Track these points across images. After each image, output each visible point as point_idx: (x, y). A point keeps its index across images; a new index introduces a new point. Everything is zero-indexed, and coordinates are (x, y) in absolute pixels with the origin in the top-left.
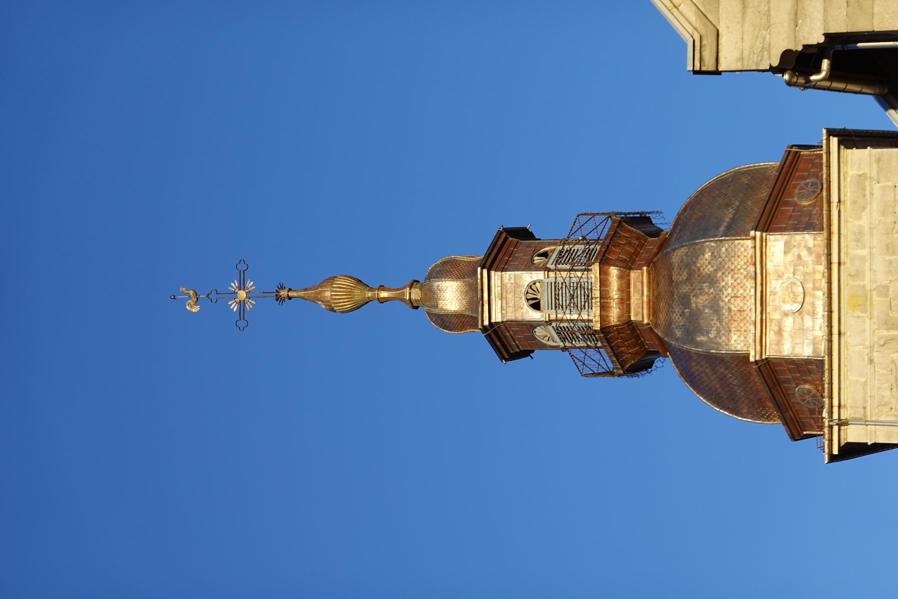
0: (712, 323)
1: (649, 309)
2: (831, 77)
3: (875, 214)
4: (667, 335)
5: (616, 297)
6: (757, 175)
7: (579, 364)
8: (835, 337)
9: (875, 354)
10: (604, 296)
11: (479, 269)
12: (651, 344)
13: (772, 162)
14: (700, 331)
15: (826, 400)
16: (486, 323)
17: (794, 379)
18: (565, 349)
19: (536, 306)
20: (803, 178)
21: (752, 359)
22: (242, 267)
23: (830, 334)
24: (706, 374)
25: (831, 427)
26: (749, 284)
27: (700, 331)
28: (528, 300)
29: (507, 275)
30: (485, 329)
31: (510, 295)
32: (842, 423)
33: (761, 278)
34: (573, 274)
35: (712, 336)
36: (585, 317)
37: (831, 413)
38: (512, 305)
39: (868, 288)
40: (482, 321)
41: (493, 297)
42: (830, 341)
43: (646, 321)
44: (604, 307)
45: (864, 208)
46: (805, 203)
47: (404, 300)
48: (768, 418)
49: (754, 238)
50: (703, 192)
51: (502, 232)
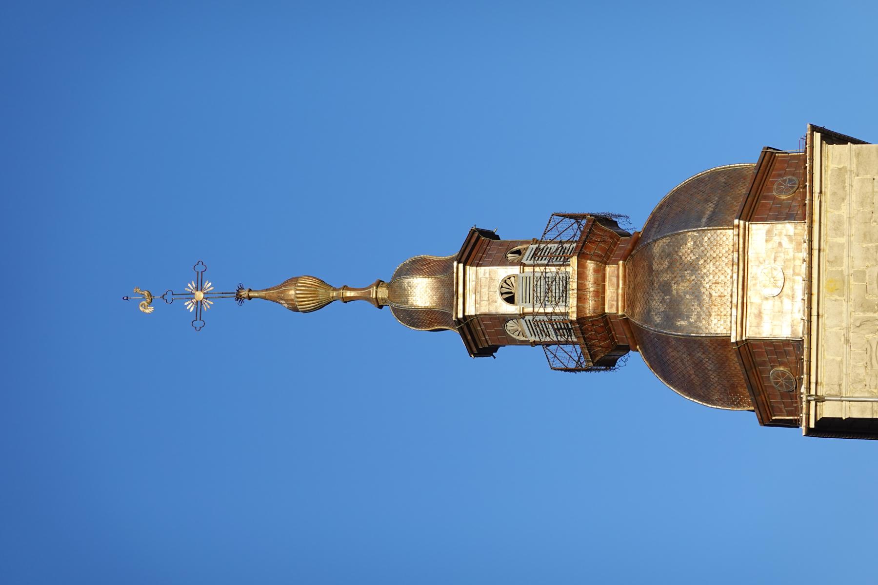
0: (693, 308)
1: (624, 301)
3: (854, 205)
4: (646, 322)
5: (592, 289)
6: (733, 176)
7: (551, 356)
8: (814, 318)
9: (851, 334)
11: (455, 263)
12: (622, 336)
13: (750, 160)
14: (680, 315)
15: (805, 377)
16: (460, 315)
17: (771, 361)
18: (534, 344)
19: (510, 300)
20: (780, 176)
21: (733, 340)
23: (810, 315)
24: (682, 361)
25: (809, 402)
28: (502, 294)
29: (481, 270)
30: (459, 321)
31: (483, 290)
32: (819, 400)
34: (548, 269)
35: (692, 320)
37: (809, 389)
38: (486, 298)
39: (846, 273)
40: (457, 313)
41: (467, 291)
42: (810, 321)
43: (620, 313)
44: (581, 299)
45: (843, 199)
46: (783, 197)
47: (369, 299)
48: (738, 405)
49: (738, 226)
50: (679, 191)
51: (474, 231)
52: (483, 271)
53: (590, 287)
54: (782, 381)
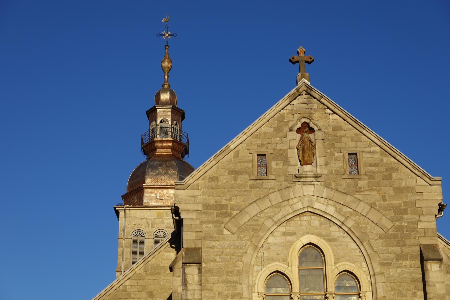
2: (176, 220)
8: (149, 208)
10: (164, 142)
14: (152, 169)
15: (131, 206)
19: (161, 122)
22: (175, 35)
23: (150, 207)
25: (123, 207)
26: (165, 184)
27: (152, 169)
29: (170, 113)
30: (155, 107)
31: (165, 114)
33: (166, 187)
36: (158, 136)
37: (128, 207)
42: (148, 207)
44: (160, 142)
48: (128, 189)
52: (170, 114)
53: (164, 145)
54: (133, 200)
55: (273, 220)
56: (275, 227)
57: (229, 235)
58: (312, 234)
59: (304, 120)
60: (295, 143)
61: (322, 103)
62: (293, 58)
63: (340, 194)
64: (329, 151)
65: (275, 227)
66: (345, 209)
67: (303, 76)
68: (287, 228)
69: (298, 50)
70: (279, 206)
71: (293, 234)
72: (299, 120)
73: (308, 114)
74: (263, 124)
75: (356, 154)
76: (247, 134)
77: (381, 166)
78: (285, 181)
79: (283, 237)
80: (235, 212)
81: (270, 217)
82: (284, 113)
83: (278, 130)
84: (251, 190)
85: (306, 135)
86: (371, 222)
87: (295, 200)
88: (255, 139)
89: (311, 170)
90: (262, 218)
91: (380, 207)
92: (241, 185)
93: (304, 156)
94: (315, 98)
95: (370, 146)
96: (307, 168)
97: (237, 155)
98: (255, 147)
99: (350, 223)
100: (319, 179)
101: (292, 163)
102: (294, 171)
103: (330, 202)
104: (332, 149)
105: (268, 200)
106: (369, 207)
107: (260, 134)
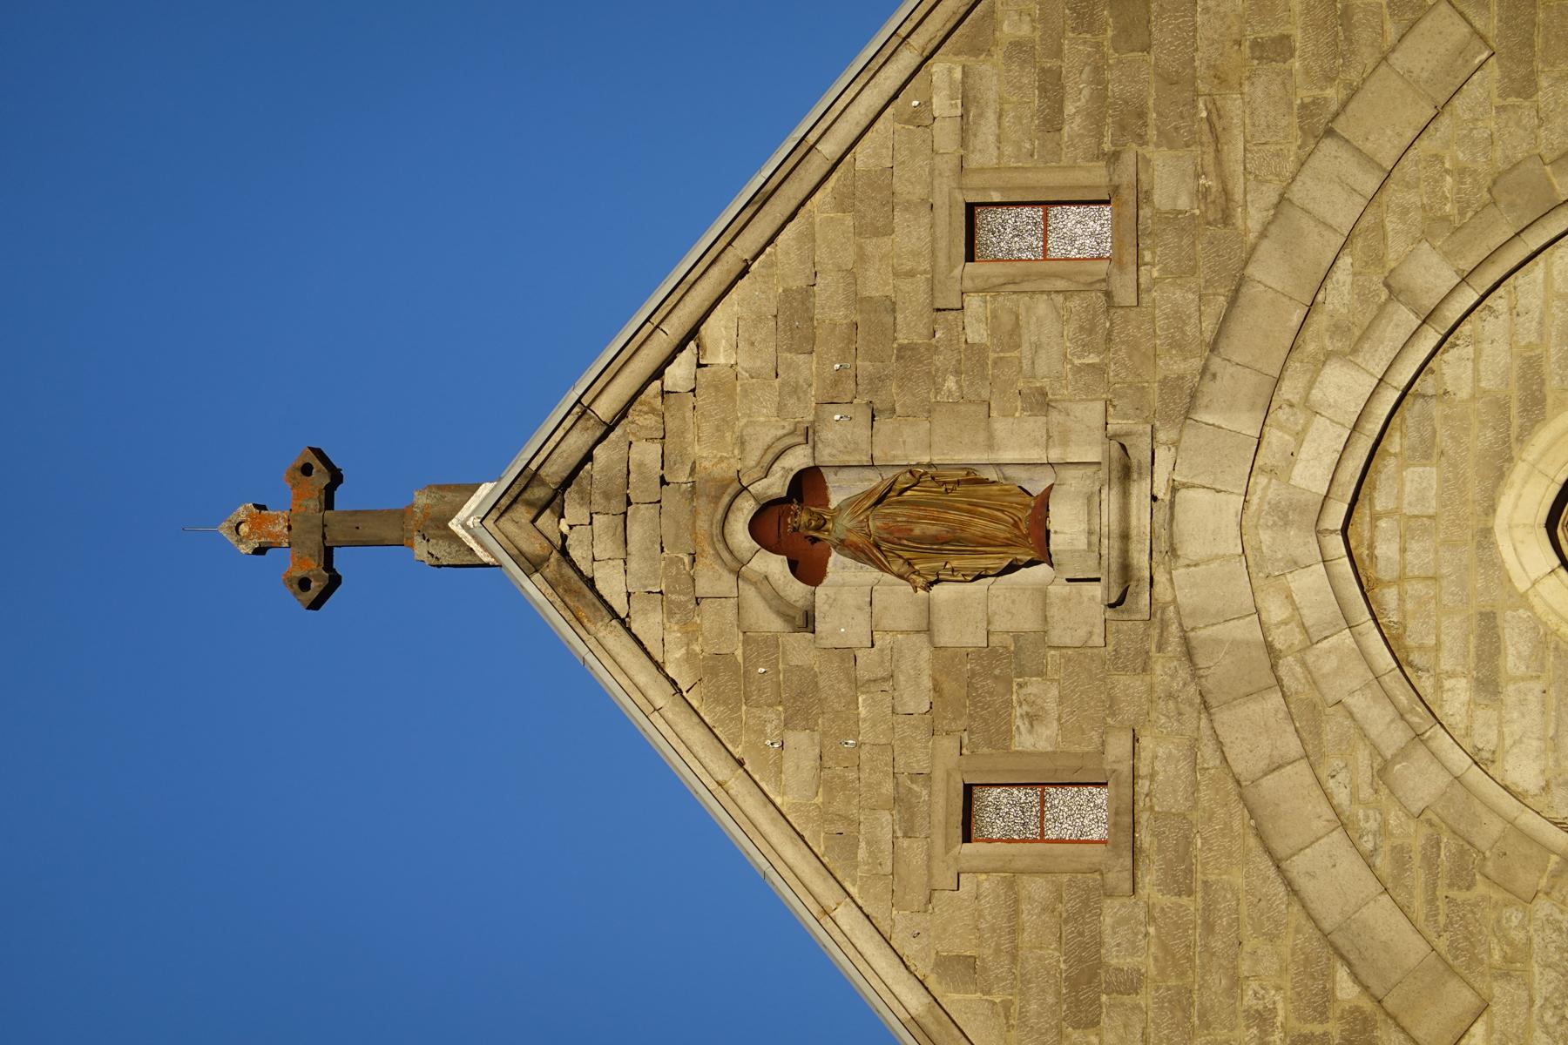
55: (1403, 754)
56: (1442, 741)
57: (1490, 1030)
58: (1491, 509)
59: (741, 537)
60: (896, 595)
61: (623, 413)
62: (304, 584)
63: (1238, 329)
64: (951, 383)
65: (1442, 741)
66: (1340, 296)
67: (438, 525)
68: (1447, 664)
69: (245, 549)
70: (1308, 716)
71: (1488, 628)
72: (738, 569)
73: (702, 503)
74: (759, 800)
75: (971, 208)
76: (830, 903)
77: (1058, 53)
78: (1145, 669)
79: (1510, 692)
80: (1346, 989)
81: (1382, 772)
82: (690, 657)
83: (801, 703)
84: (1199, 886)
85: (843, 526)
86: (1424, 144)
87: (1275, 611)
88: (862, 853)
89: (1080, 503)
90: (1384, 824)
91: (1329, 78)
92: (1164, 947)
93: (983, 544)
94: (588, 457)
95: (921, 119)
96: (1067, 526)
97: (963, 969)
98: (914, 851)
99: (1432, 273)
100: (1139, 453)
101: (1027, 621)
102: (1080, 613)
103: (1290, 390)
104: (939, 360)
105: (1267, 782)
106: (1328, 146)
107: (825, 816)
